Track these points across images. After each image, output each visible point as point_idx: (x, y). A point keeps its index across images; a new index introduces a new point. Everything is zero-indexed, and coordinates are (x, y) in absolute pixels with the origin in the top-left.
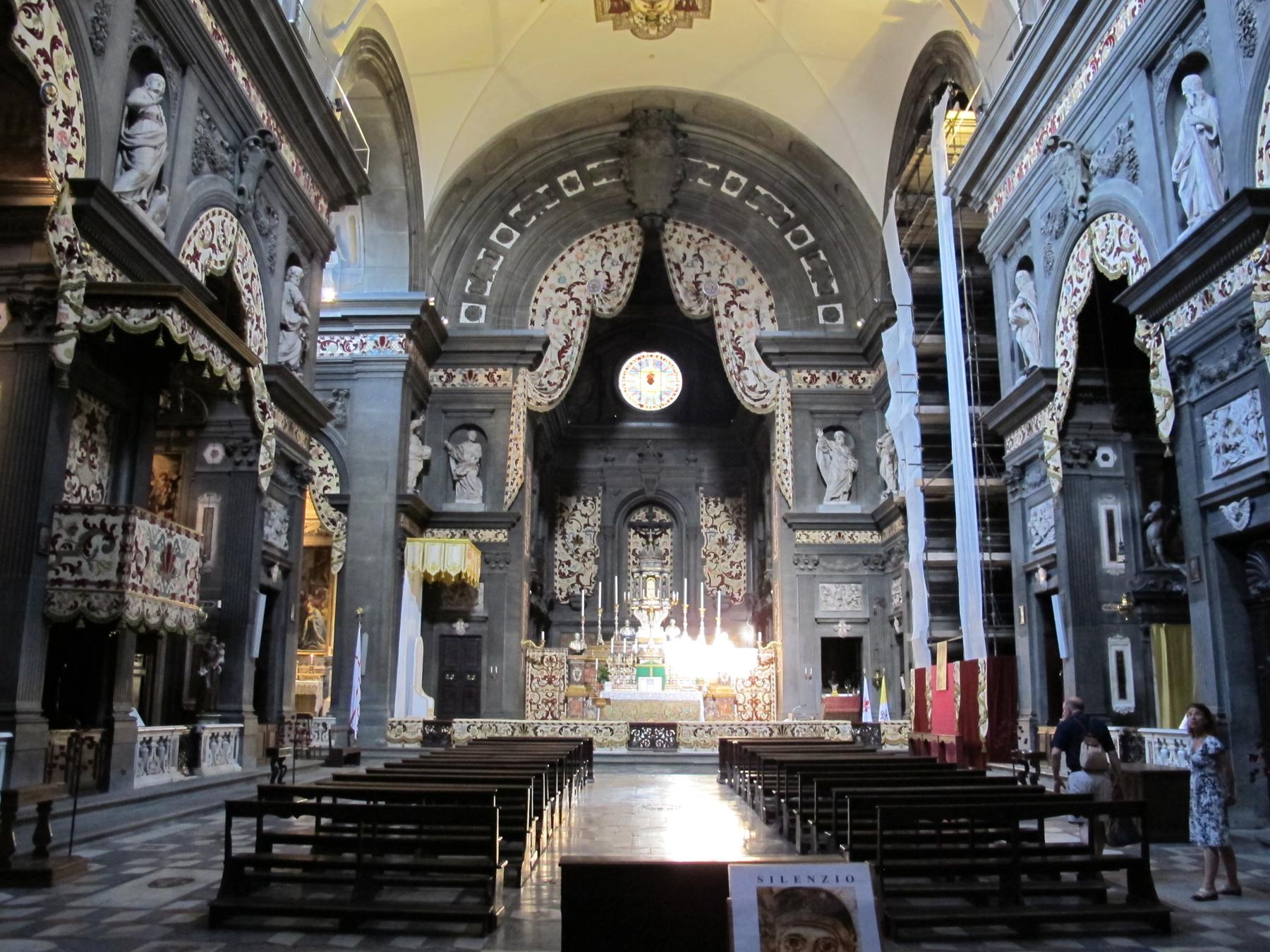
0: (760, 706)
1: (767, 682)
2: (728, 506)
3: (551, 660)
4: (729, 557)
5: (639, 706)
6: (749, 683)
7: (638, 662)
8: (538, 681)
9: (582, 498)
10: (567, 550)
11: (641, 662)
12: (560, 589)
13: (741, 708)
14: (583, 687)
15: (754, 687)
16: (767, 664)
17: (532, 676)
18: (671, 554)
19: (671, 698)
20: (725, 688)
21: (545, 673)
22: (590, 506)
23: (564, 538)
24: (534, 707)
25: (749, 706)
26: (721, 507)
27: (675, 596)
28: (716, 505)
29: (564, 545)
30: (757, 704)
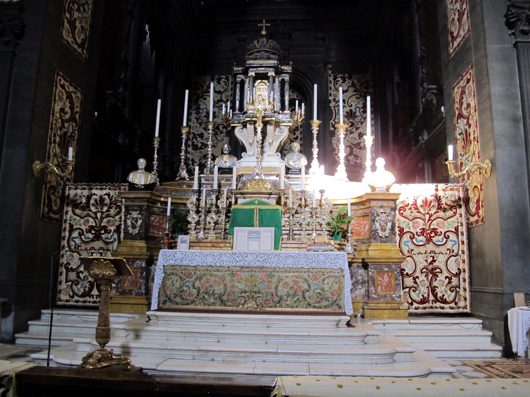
0: (441, 277)
1: (453, 237)
2: (356, 82)
3: (102, 199)
4: (357, 129)
5: (228, 278)
6: (422, 239)
7: (236, 202)
8: (80, 235)
9: (216, 77)
10: (200, 124)
11: (240, 201)
12: (193, 160)
13: (409, 282)
14: (142, 244)
15: (430, 247)
16: (451, 207)
17: (71, 226)
18: (301, 130)
19: (290, 263)
20: (388, 246)
21: (92, 222)
22: (223, 84)
23: (198, 113)
24: (73, 276)
25: (422, 277)
26: (348, 82)
27: (300, 111)
28: (344, 81)
29: (197, 119)
30: (435, 275)
